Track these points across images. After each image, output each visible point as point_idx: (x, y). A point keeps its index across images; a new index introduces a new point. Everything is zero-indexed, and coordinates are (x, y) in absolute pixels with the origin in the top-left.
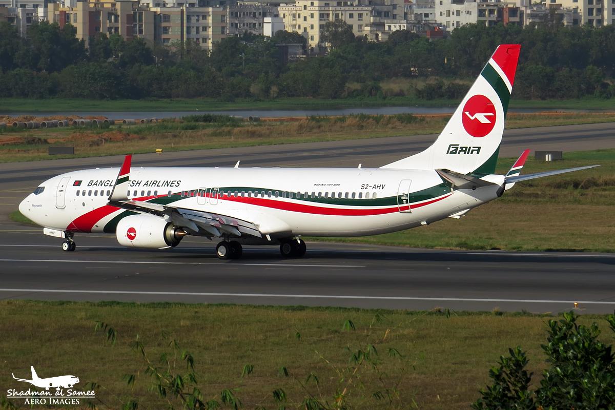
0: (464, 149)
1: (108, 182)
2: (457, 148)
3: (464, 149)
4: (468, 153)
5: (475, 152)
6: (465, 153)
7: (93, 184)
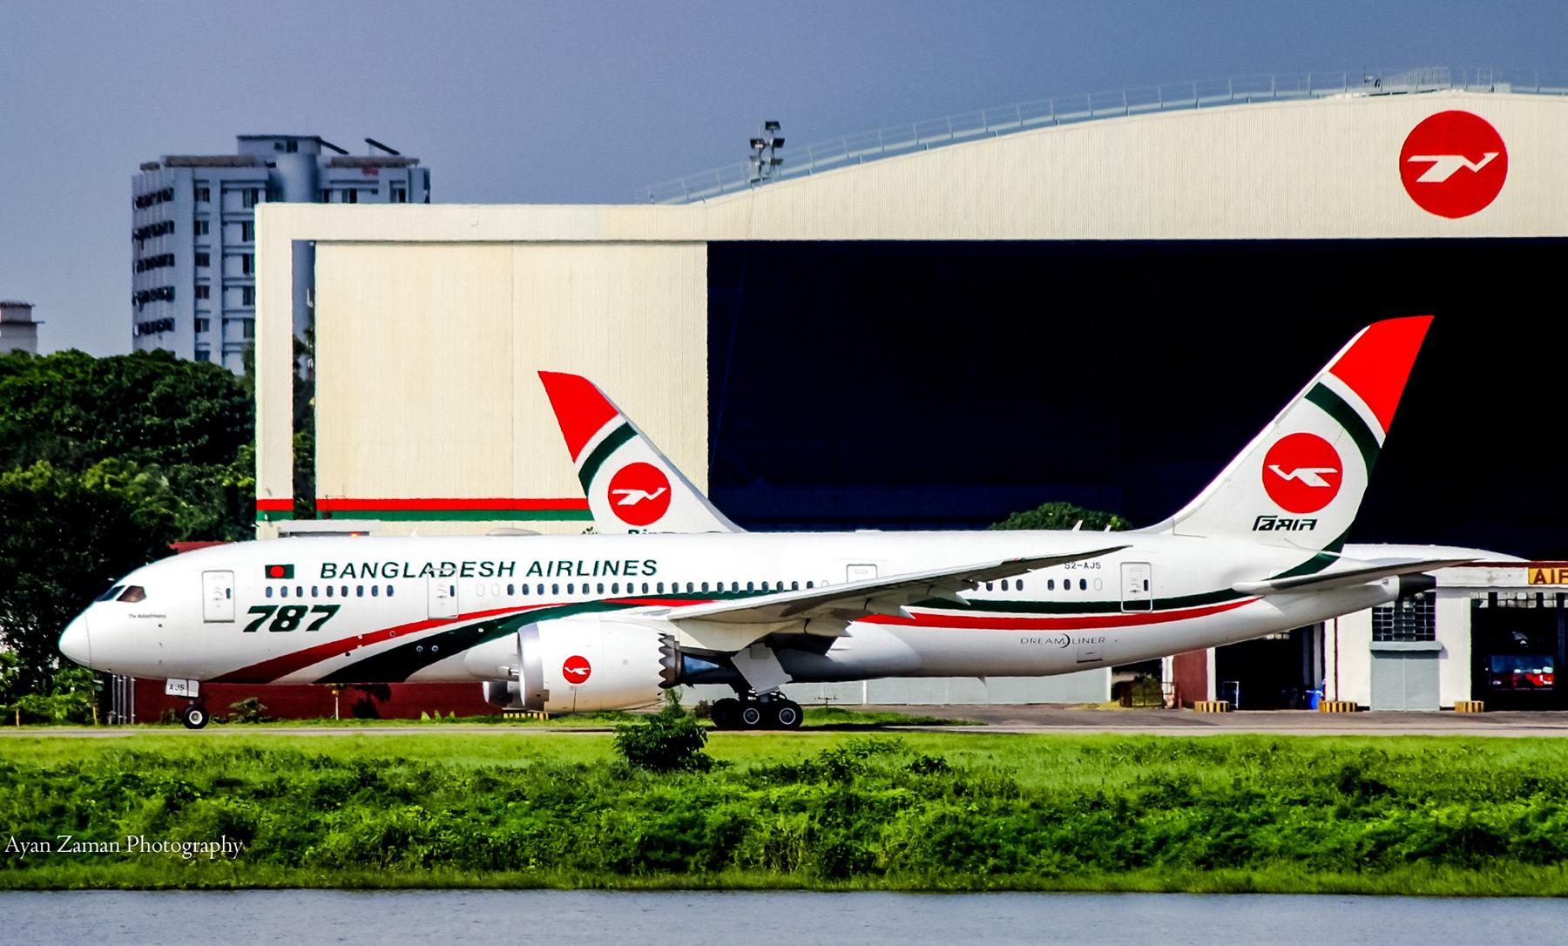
0: (1287, 523)
1: (394, 567)
2: (1272, 523)
3: (1287, 523)
4: (1294, 529)
6: (1288, 529)
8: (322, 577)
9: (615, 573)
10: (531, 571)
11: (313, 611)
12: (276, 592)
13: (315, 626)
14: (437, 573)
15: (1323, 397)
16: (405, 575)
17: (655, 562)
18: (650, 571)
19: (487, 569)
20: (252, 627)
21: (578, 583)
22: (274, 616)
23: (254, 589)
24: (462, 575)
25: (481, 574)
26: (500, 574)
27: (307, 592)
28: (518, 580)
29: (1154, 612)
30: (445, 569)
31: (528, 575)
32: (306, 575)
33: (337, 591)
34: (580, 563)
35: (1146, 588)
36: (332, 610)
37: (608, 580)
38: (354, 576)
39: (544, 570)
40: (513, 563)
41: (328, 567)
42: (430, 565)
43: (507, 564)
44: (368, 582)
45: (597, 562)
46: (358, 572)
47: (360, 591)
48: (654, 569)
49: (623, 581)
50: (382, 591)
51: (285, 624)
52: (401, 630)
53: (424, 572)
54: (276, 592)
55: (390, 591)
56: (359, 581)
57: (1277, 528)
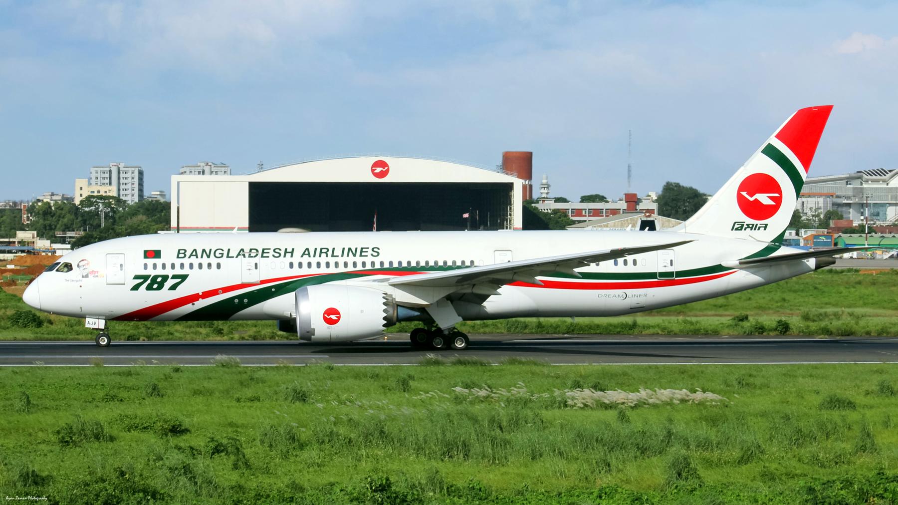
0: (751, 226)
1: (221, 252)
2: (743, 225)
3: (751, 226)
4: (755, 229)
5: (762, 229)
6: (751, 230)
7: (188, 254)
8: (178, 257)
9: (355, 255)
10: (304, 254)
11: (171, 278)
12: (150, 266)
13: (173, 287)
14: (247, 255)
15: (771, 152)
16: (228, 257)
17: (379, 249)
18: (375, 254)
19: (277, 253)
20: (136, 288)
21: (332, 261)
22: (149, 281)
23: (138, 265)
24: (262, 256)
25: (273, 256)
26: (285, 256)
27: (168, 266)
28: (296, 259)
29: (676, 279)
30: (253, 252)
31: (302, 256)
32: (169, 256)
33: (187, 266)
34: (334, 249)
35: (671, 265)
36: (184, 278)
37: (350, 259)
38: (197, 257)
39: (312, 253)
40: (293, 249)
41: (181, 252)
42: (242, 250)
43: (289, 250)
44: (205, 261)
45: (344, 249)
46: (199, 254)
47: (200, 266)
48: (378, 253)
49: (359, 260)
50: (214, 266)
51: (155, 286)
52: (226, 290)
53: (239, 254)
54: (150, 266)
55: (219, 266)
56: (200, 260)
57: (745, 229)
